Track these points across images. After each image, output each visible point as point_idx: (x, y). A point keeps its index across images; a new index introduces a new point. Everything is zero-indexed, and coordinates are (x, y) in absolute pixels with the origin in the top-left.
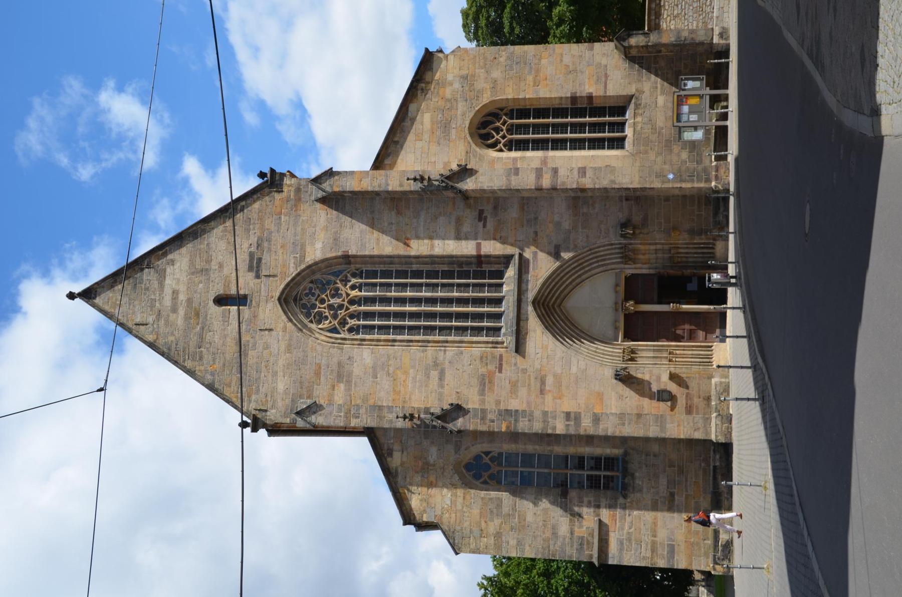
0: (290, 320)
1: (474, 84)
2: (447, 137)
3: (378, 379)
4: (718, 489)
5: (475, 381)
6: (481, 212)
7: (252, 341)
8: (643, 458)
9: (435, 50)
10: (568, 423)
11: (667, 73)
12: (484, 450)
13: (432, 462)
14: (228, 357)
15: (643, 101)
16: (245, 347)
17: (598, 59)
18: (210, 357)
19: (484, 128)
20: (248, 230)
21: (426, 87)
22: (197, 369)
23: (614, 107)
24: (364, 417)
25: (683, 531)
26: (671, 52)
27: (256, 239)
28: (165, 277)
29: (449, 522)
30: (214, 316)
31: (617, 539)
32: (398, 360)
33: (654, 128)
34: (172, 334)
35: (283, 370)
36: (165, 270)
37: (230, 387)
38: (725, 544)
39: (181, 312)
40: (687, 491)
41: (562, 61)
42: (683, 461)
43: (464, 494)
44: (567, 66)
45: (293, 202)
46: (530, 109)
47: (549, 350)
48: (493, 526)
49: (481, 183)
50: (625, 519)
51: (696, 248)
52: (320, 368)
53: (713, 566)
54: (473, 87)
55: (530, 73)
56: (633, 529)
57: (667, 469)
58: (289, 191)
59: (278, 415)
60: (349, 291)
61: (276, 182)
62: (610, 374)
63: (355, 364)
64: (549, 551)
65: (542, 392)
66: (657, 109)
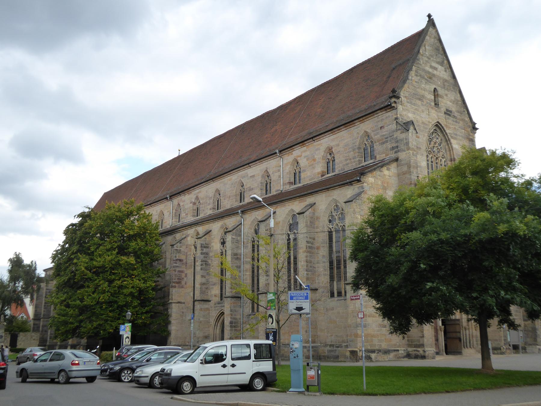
4: (391, 353)
14: (418, 90)
34: (423, 63)
38: (370, 357)
39: (430, 70)
58: (471, 136)
63: (421, 157)
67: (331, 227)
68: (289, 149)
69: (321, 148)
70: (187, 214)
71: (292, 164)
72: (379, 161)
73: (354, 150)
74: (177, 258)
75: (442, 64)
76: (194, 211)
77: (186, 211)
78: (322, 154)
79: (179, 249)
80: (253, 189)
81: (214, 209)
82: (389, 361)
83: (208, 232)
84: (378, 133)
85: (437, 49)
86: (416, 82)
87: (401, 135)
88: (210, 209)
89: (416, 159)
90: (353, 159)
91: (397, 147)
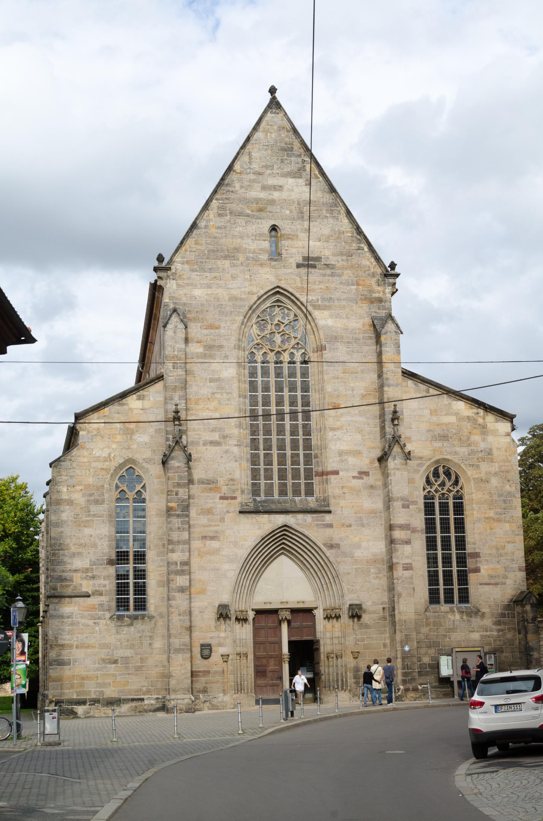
0: (259, 299)
1: (484, 461)
2: (434, 439)
3: (209, 384)
4: (123, 703)
5: (210, 475)
6: (367, 474)
7: (239, 262)
8: (148, 634)
9: (514, 424)
10: (179, 563)
11: (500, 640)
12: (147, 485)
13: (134, 437)
14: (223, 241)
15: (473, 620)
16: (233, 257)
17: (511, 575)
18: (222, 224)
19: (444, 473)
20: (342, 254)
21: (480, 417)
22: (210, 212)
23: (467, 593)
24: (175, 374)
25: (83, 673)
26: (520, 643)
27: (333, 263)
28: (294, 177)
29: (79, 456)
30: (260, 226)
31: (73, 613)
32: (227, 402)
33: (450, 630)
34: (242, 187)
35: (213, 294)
36: (301, 177)
37: (195, 244)
38: (73, 711)
39: (263, 195)
40: (120, 675)
41: (509, 542)
42: (147, 670)
43: (106, 469)
44: (504, 548)
45: (368, 296)
46: (463, 514)
47: (243, 543)
48: (78, 497)
49: (394, 474)
50: (91, 619)
51: (342, 674)
52: (217, 328)
53: (53, 701)
54: (481, 460)
55: (497, 513)
56: (82, 627)
57: (139, 656)
58: (379, 292)
59: (171, 291)
60: (287, 351)
61: (386, 279)
62: (223, 600)
64: (59, 550)
65: (204, 538)
66: (468, 632)
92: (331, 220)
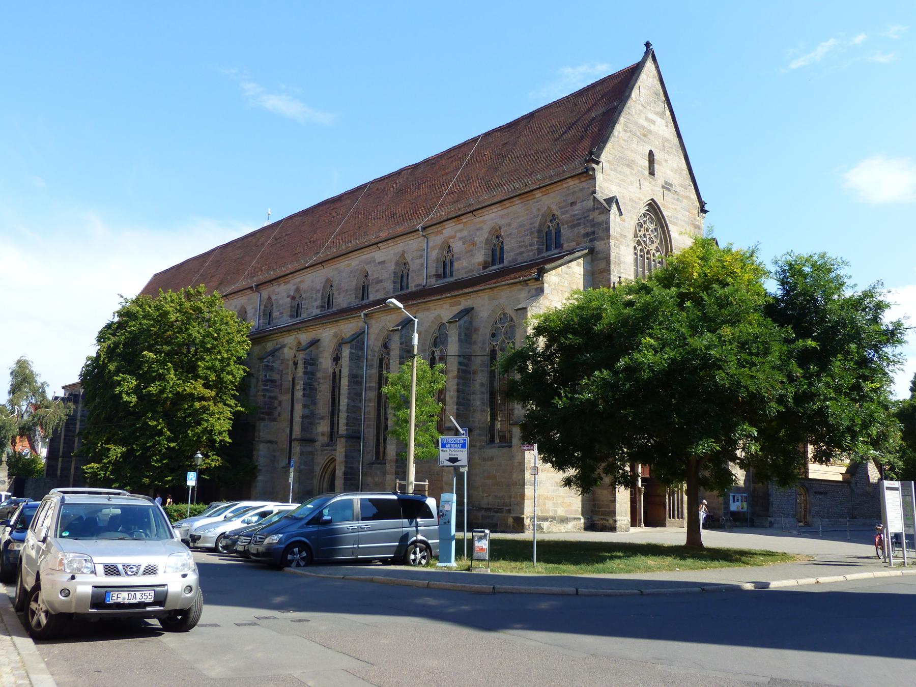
14: (626, 152)
34: (636, 113)
39: (646, 124)
67: (494, 344)
68: (438, 226)
69: (485, 227)
70: (281, 313)
71: (441, 248)
72: (567, 251)
73: (532, 233)
74: (268, 377)
75: (662, 115)
76: (293, 309)
77: (281, 308)
78: (486, 237)
79: (270, 364)
80: (381, 281)
81: (322, 307)
82: (566, 532)
83: (315, 342)
84: (567, 211)
85: (657, 94)
86: (624, 140)
87: (599, 216)
88: (317, 308)
89: (618, 252)
90: (531, 246)
91: (593, 233)
92: (677, 159)
